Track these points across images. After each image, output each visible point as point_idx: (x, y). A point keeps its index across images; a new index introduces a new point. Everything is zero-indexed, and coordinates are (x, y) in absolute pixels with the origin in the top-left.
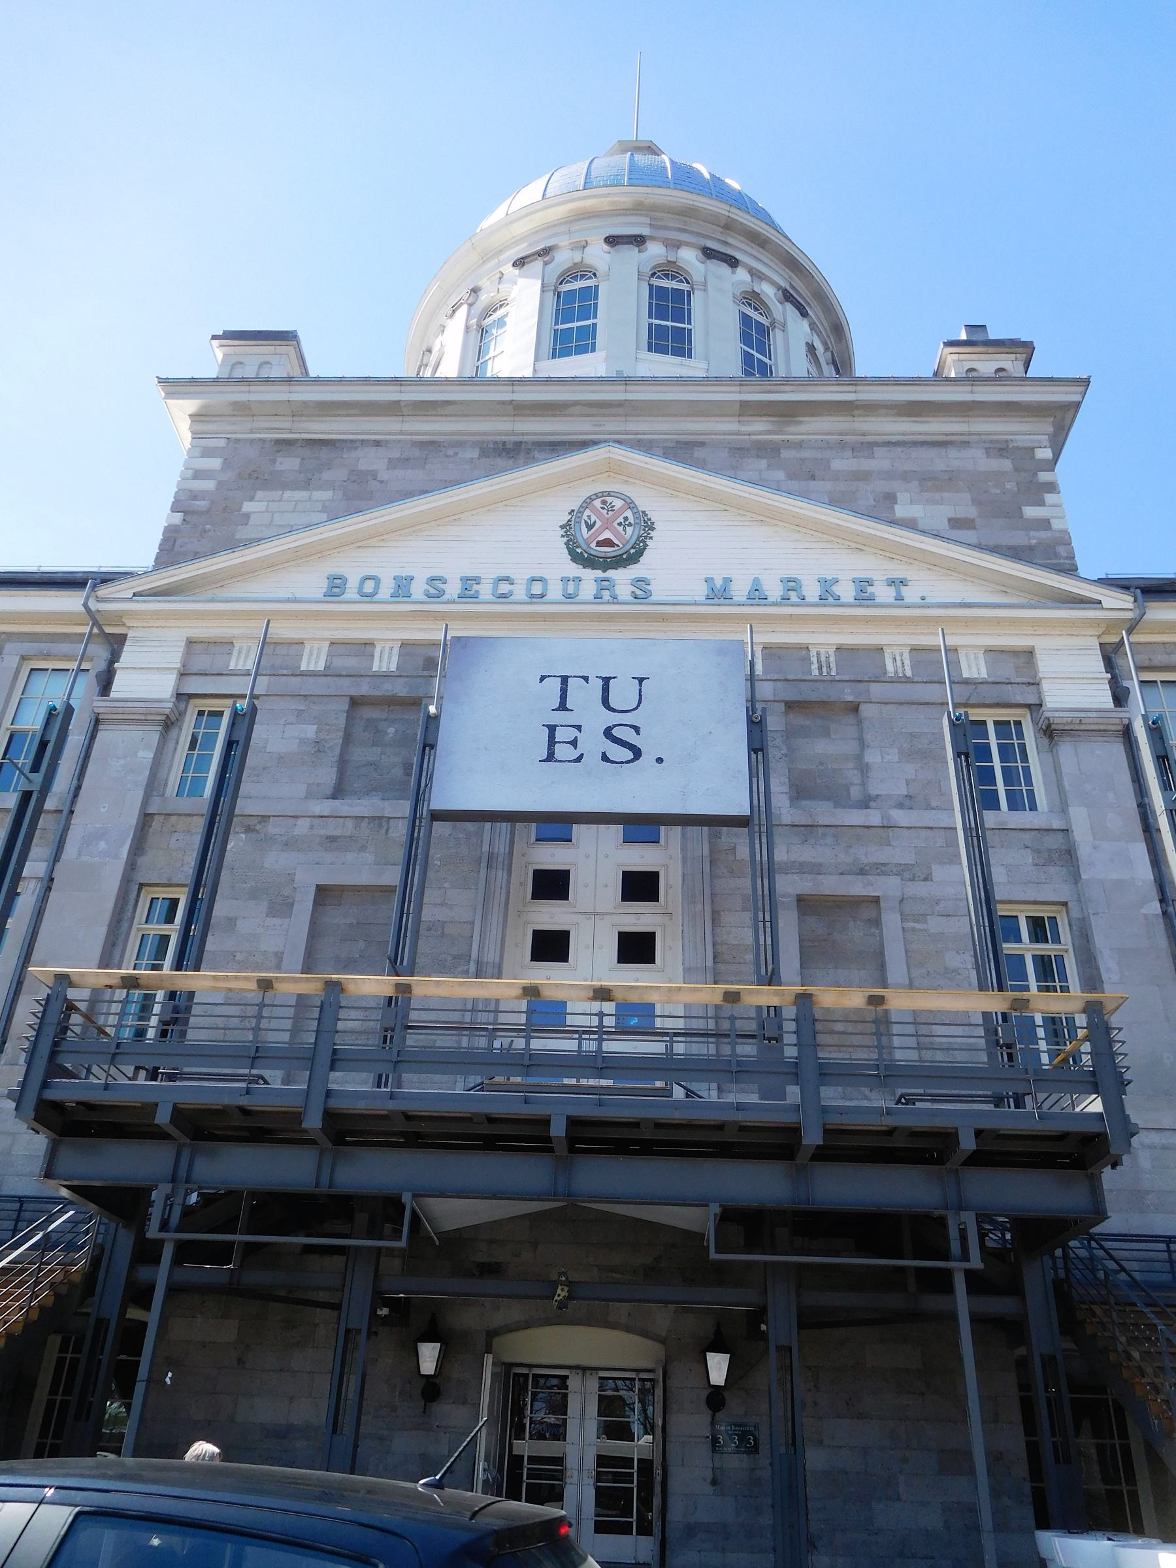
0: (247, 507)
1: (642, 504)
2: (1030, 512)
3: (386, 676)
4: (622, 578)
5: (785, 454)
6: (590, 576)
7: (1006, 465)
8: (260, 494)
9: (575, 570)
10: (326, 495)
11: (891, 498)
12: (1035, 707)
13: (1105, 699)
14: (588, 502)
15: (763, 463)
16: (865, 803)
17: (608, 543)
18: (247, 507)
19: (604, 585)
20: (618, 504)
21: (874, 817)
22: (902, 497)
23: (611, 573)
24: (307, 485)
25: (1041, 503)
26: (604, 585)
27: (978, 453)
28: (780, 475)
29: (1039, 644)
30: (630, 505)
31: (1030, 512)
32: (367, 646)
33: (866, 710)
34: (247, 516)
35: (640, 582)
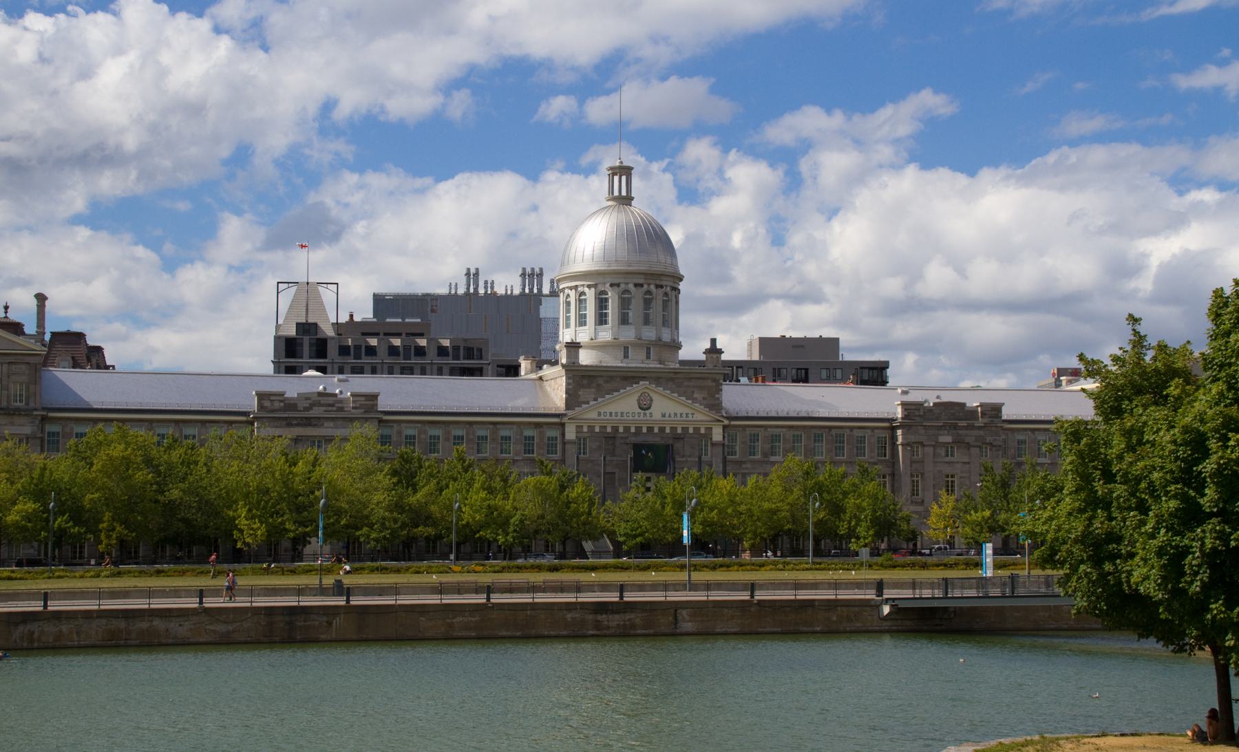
0: (580, 393)
1: (651, 395)
2: (717, 396)
4: (648, 412)
5: (676, 381)
6: (642, 412)
7: (714, 384)
8: (581, 390)
9: (640, 411)
10: (593, 390)
11: (693, 392)
12: (711, 439)
13: (722, 439)
14: (640, 397)
16: (683, 456)
17: (645, 404)
18: (580, 393)
19: (645, 414)
20: (647, 395)
21: (684, 459)
22: (696, 392)
23: (647, 411)
25: (718, 394)
26: (645, 414)
27: (710, 381)
28: (674, 386)
29: (713, 427)
30: (649, 395)
31: (717, 396)
32: (605, 427)
33: (685, 439)
35: (651, 413)
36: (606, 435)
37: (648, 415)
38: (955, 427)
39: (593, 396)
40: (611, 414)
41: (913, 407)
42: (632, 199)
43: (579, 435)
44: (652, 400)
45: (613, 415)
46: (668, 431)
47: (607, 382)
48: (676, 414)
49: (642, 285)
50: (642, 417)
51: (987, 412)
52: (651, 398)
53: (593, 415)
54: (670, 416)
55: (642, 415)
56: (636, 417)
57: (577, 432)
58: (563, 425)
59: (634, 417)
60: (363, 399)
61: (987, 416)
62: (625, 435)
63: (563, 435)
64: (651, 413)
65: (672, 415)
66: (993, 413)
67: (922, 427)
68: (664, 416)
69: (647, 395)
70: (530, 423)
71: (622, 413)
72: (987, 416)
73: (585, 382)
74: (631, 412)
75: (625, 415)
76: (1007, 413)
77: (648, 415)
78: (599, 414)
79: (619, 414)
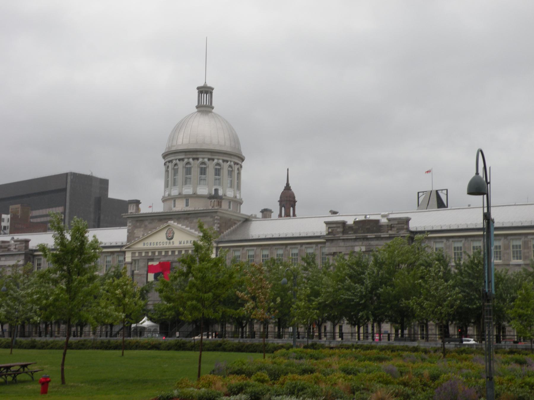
0: (135, 231)
1: (173, 230)
3: (150, 256)
4: (171, 241)
6: (168, 241)
7: (212, 219)
9: (167, 240)
10: (142, 229)
15: (187, 221)
19: (170, 243)
24: (140, 227)
26: (170, 243)
28: (188, 223)
30: (172, 230)
34: (135, 233)
36: (148, 258)
37: (171, 243)
38: (366, 239)
39: (142, 233)
40: (150, 244)
41: (334, 225)
42: (213, 108)
43: (134, 258)
44: (174, 233)
45: (152, 244)
46: (183, 252)
47: (150, 223)
48: (187, 242)
49: (182, 160)
50: (168, 245)
51: (395, 225)
52: (173, 232)
53: (140, 246)
54: (184, 243)
55: (168, 243)
56: (165, 245)
57: (132, 257)
58: (124, 252)
59: (164, 244)
60: (19, 243)
61: (395, 229)
62: (159, 257)
63: (125, 258)
64: (173, 242)
65: (186, 242)
66: (400, 225)
67: (342, 241)
68: (180, 243)
69: (171, 230)
70: (108, 252)
71: (157, 243)
72: (395, 229)
73: (138, 224)
74: (162, 242)
75: (158, 244)
76: (413, 226)
77: (171, 243)
78: (144, 244)
79: (155, 244)
